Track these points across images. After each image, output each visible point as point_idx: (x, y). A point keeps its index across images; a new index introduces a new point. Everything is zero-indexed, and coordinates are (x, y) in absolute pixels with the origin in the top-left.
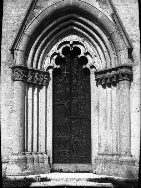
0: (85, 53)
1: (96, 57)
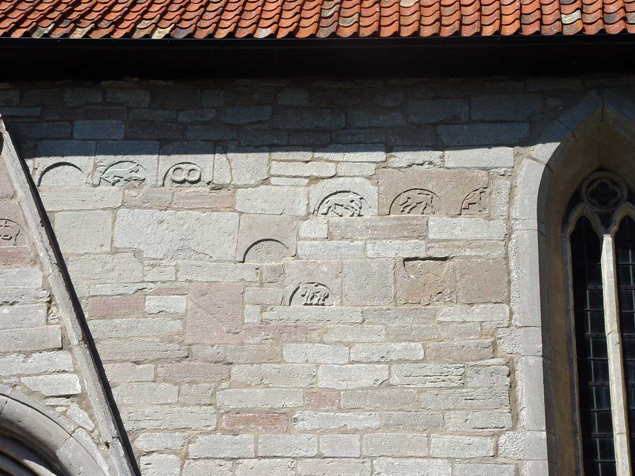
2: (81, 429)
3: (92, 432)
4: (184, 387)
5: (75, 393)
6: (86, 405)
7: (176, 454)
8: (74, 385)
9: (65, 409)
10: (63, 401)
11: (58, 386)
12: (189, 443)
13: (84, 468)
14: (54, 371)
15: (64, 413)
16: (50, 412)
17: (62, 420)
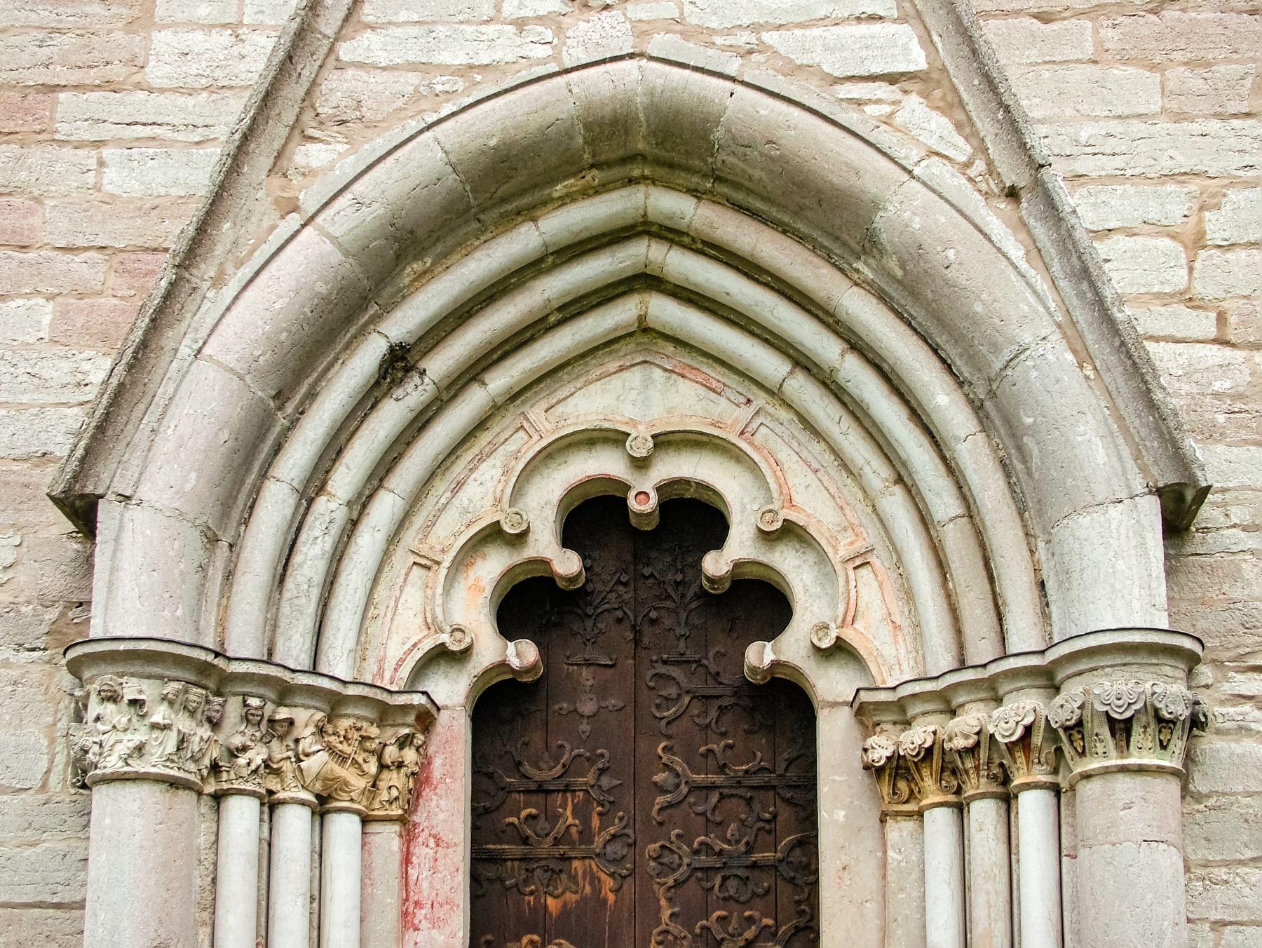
0: (768, 538)
1: (864, 571)
2: (936, 158)
3: (968, 164)
4: (1177, 75)
5: (912, 68)
6: (943, 98)
7: (1173, 237)
8: (906, 49)
9: (887, 109)
10: (882, 90)
11: (864, 53)
12: (1201, 209)
13: (958, 252)
14: (846, 15)
15: (887, 120)
16: (849, 117)
17: (884, 137)
